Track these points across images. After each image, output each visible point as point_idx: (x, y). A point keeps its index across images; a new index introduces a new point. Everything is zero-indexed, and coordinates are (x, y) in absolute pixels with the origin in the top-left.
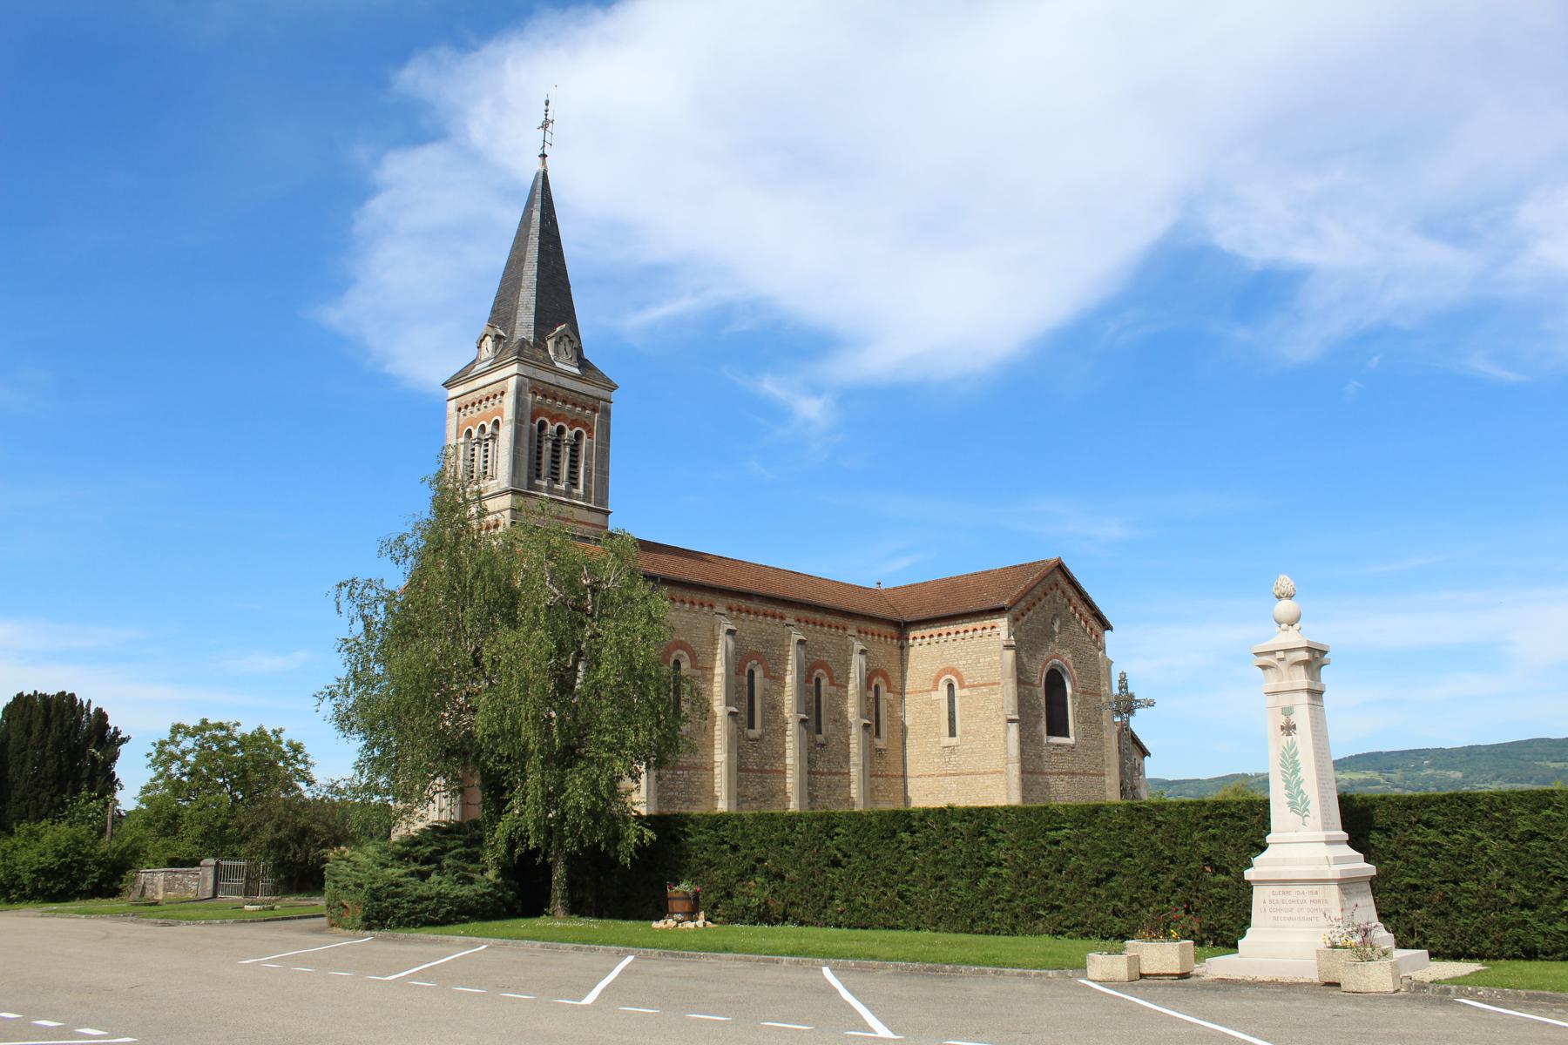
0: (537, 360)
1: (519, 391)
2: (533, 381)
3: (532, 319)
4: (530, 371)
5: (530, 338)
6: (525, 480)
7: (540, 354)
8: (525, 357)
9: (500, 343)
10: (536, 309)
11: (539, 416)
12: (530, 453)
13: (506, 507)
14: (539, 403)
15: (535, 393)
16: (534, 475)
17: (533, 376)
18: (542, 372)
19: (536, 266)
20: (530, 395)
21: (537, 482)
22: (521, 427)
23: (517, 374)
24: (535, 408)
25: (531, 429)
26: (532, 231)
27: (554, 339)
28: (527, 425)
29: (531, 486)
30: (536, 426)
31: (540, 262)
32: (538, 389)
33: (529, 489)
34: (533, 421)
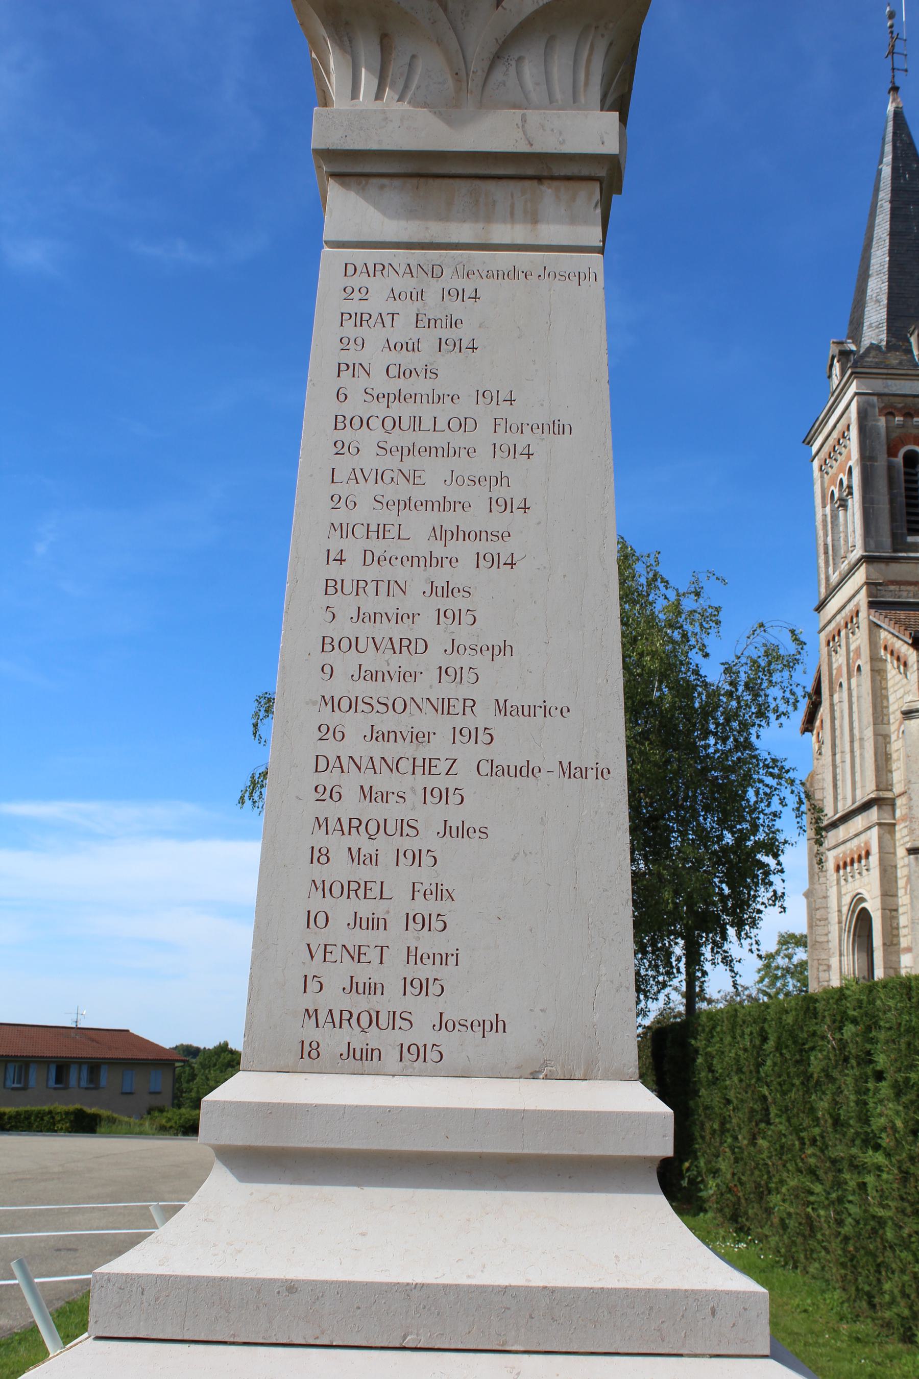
0: (887, 367)
1: (863, 416)
2: (886, 398)
3: (883, 314)
4: (878, 385)
5: (881, 340)
6: (887, 540)
7: (894, 359)
8: (870, 367)
9: (848, 360)
10: (890, 298)
11: (904, 445)
12: (892, 501)
13: (860, 585)
14: (899, 426)
15: (890, 413)
16: (905, 531)
17: (886, 391)
18: (897, 382)
19: (887, 241)
20: (883, 419)
21: (910, 539)
22: (872, 466)
23: (856, 394)
24: (894, 435)
25: (890, 468)
26: (881, 195)
27: (916, 333)
28: (882, 461)
29: (898, 543)
30: (899, 460)
31: (893, 234)
32: (895, 408)
33: (895, 551)
34: (892, 452)
